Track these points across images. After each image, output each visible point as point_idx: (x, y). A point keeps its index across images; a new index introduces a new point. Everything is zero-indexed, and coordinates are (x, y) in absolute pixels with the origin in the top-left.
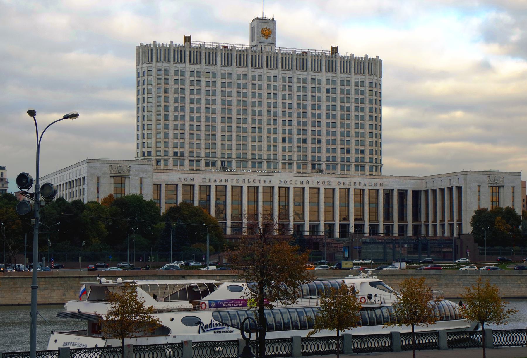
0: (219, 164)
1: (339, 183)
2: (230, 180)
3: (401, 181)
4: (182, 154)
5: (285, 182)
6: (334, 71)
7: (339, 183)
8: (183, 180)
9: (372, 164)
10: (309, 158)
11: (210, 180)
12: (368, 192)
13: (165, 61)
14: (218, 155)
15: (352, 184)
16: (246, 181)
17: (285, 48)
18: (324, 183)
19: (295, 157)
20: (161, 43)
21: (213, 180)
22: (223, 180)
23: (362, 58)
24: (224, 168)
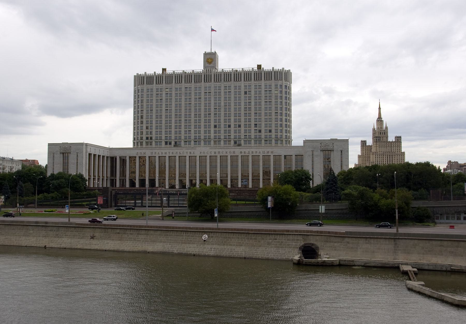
0: (173, 143)
1: (241, 152)
3: (287, 149)
4: (151, 138)
6: (250, 80)
7: (241, 152)
8: (139, 154)
9: (276, 139)
11: (155, 153)
12: (209, 157)
13: (142, 84)
14: (173, 138)
15: (251, 152)
16: (178, 153)
17: (228, 69)
18: (230, 153)
19: (222, 137)
20: (267, 69)
21: (157, 153)
22: (164, 153)
23: (280, 70)
24: (176, 145)
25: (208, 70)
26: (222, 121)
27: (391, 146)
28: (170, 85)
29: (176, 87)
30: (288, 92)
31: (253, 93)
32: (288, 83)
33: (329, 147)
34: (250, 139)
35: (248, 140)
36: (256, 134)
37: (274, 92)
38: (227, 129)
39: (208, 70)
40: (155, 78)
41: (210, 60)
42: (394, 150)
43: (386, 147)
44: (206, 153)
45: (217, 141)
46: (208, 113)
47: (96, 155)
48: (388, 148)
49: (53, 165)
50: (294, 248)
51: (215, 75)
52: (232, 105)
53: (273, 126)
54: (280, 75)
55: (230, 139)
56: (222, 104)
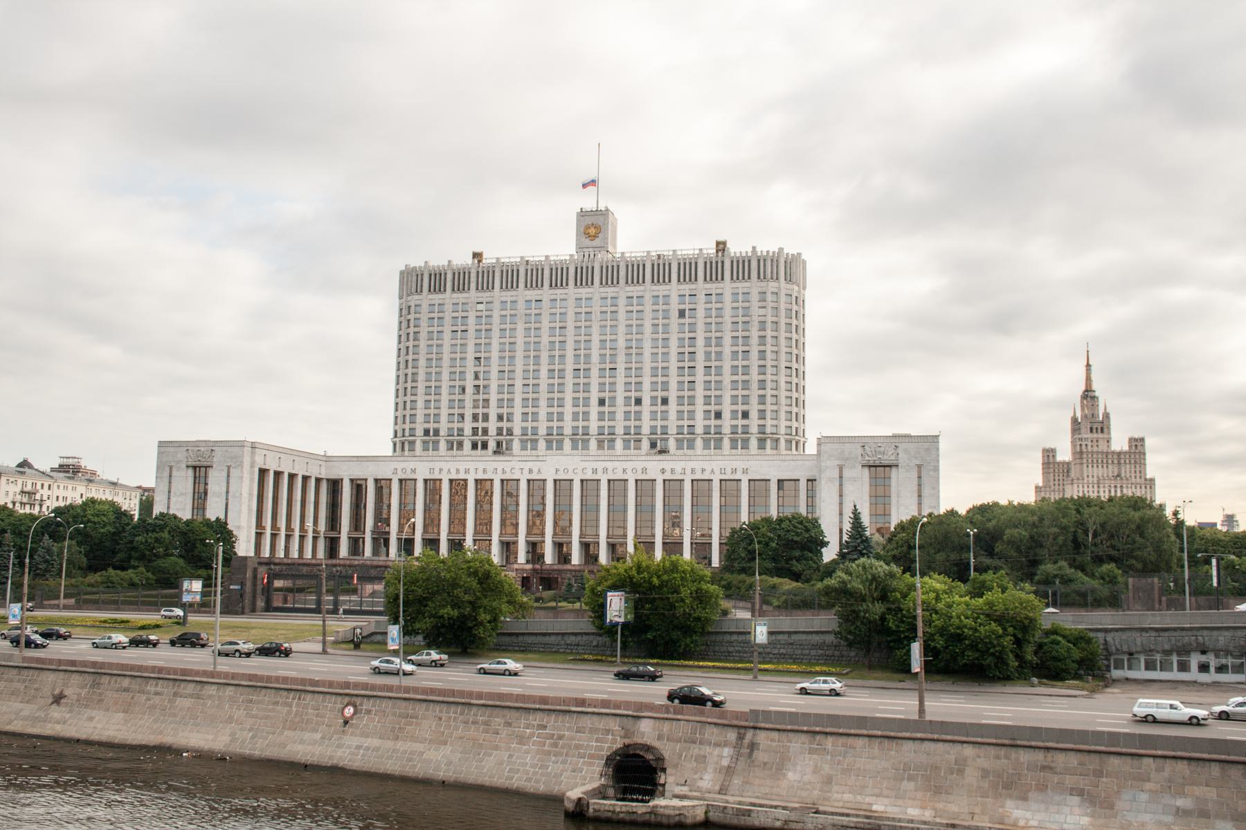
0: (492, 445)
1: (663, 471)
2: (472, 471)
3: (786, 463)
4: (437, 432)
5: (566, 471)
7: (663, 471)
8: (399, 472)
9: (762, 436)
10: (646, 430)
11: (441, 470)
15: (688, 471)
16: (500, 471)
19: (620, 430)
22: (462, 471)
25: (587, 256)
26: (620, 387)
27: (1119, 463)
28: (488, 294)
29: (503, 299)
30: (794, 313)
31: (701, 313)
32: (796, 288)
33: (886, 457)
34: (692, 436)
35: (687, 440)
36: (707, 422)
37: (756, 312)
38: (633, 408)
39: (587, 256)
40: (449, 277)
41: (592, 231)
42: (1125, 472)
43: (1105, 466)
44: (571, 471)
45: (606, 440)
46: (608, 366)
47: (282, 473)
48: (1110, 466)
49: (169, 498)
50: (591, 756)
51: (602, 267)
52: (647, 345)
53: (754, 400)
54: (772, 266)
55: (639, 436)
56: (621, 343)
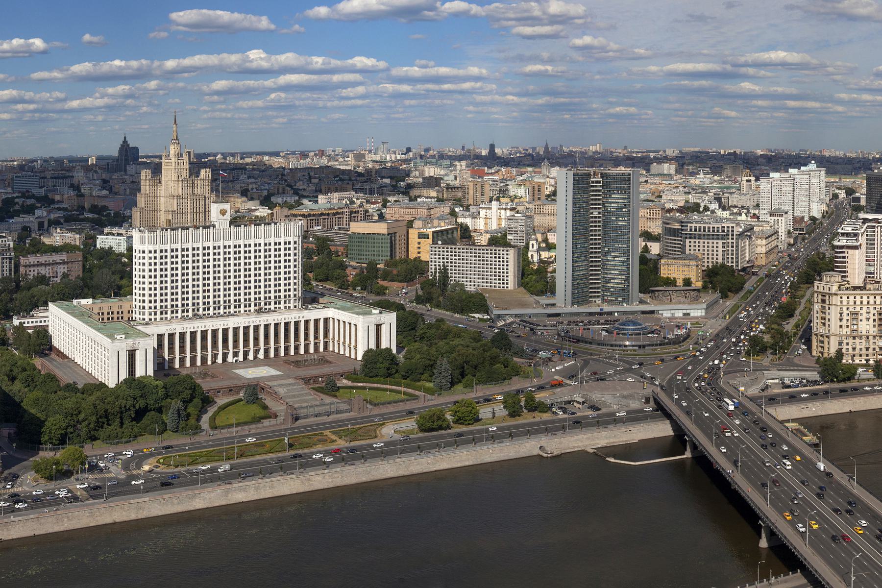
1: (274, 320)
